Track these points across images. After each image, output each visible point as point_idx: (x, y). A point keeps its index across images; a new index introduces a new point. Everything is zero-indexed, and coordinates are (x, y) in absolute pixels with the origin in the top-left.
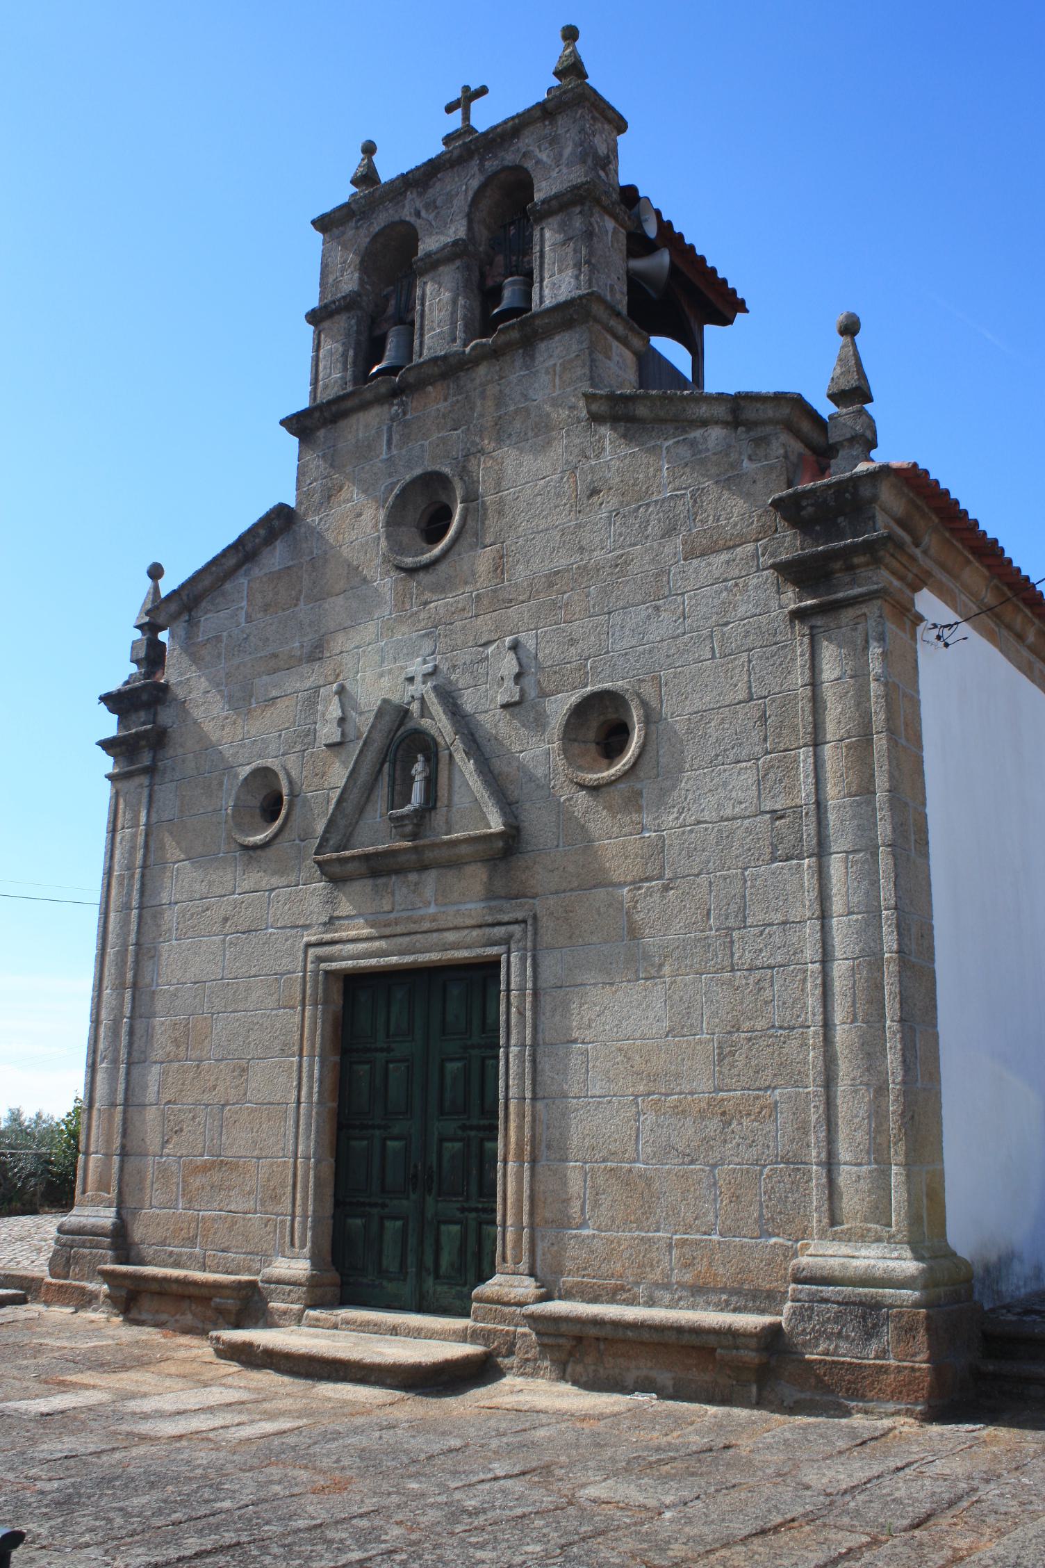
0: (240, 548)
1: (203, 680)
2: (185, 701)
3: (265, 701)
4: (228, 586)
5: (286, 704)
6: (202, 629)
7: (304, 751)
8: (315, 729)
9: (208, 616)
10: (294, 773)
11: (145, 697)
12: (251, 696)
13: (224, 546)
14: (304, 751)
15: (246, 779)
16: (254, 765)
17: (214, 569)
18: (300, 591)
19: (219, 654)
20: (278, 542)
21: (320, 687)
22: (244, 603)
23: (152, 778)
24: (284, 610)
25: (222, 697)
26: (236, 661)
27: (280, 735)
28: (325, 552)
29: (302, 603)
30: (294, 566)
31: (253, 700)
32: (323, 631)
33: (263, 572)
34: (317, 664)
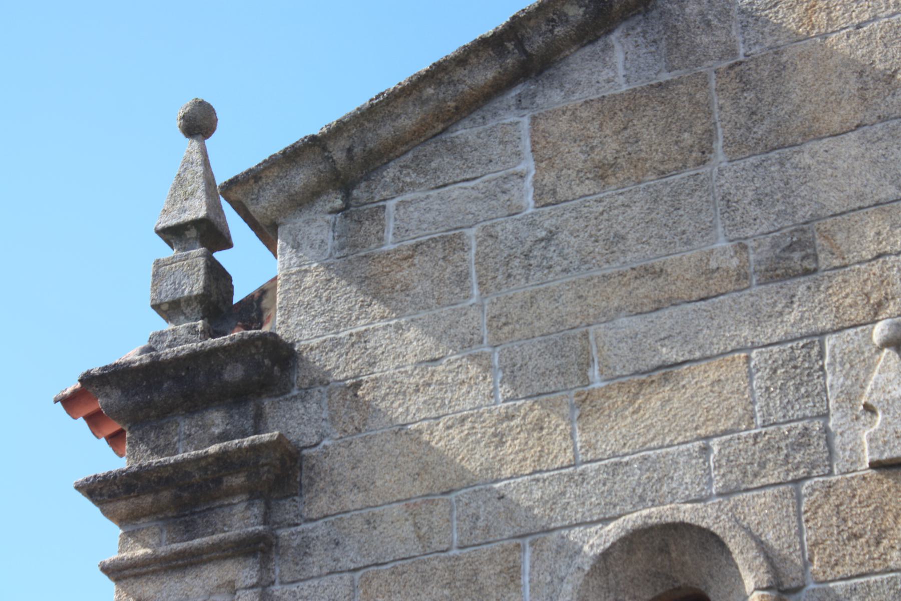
0: (510, 46)
1: (410, 334)
2: (357, 385)
3: (636, 373)
4: (464, 132)
5: (713, 375)
6: (391, 226)
7: (797, 481)
8: (826, 430)
9: (408, 196)
10: (770, 537)
11: (234, 373)
12: (585, 364)
13: (468, 38)
14: (797, 481)
15: (605, 555)
16: (634, 519)
17: (430, 91)
18: (710, 134)
19: (462, 278)
20: (614, 38)
21: (823, 333)
22: (528, 165)
23: (265, 565)
24: (662, 174)
25: (487, 368)
26: (520, 290)
27: (706, 450)
28: (777, 51)
29: (720, 156)
30: (680, 81)
31: (594, 372)
32: (804, 213)
33: (577, 98)
34: (801, 287)
